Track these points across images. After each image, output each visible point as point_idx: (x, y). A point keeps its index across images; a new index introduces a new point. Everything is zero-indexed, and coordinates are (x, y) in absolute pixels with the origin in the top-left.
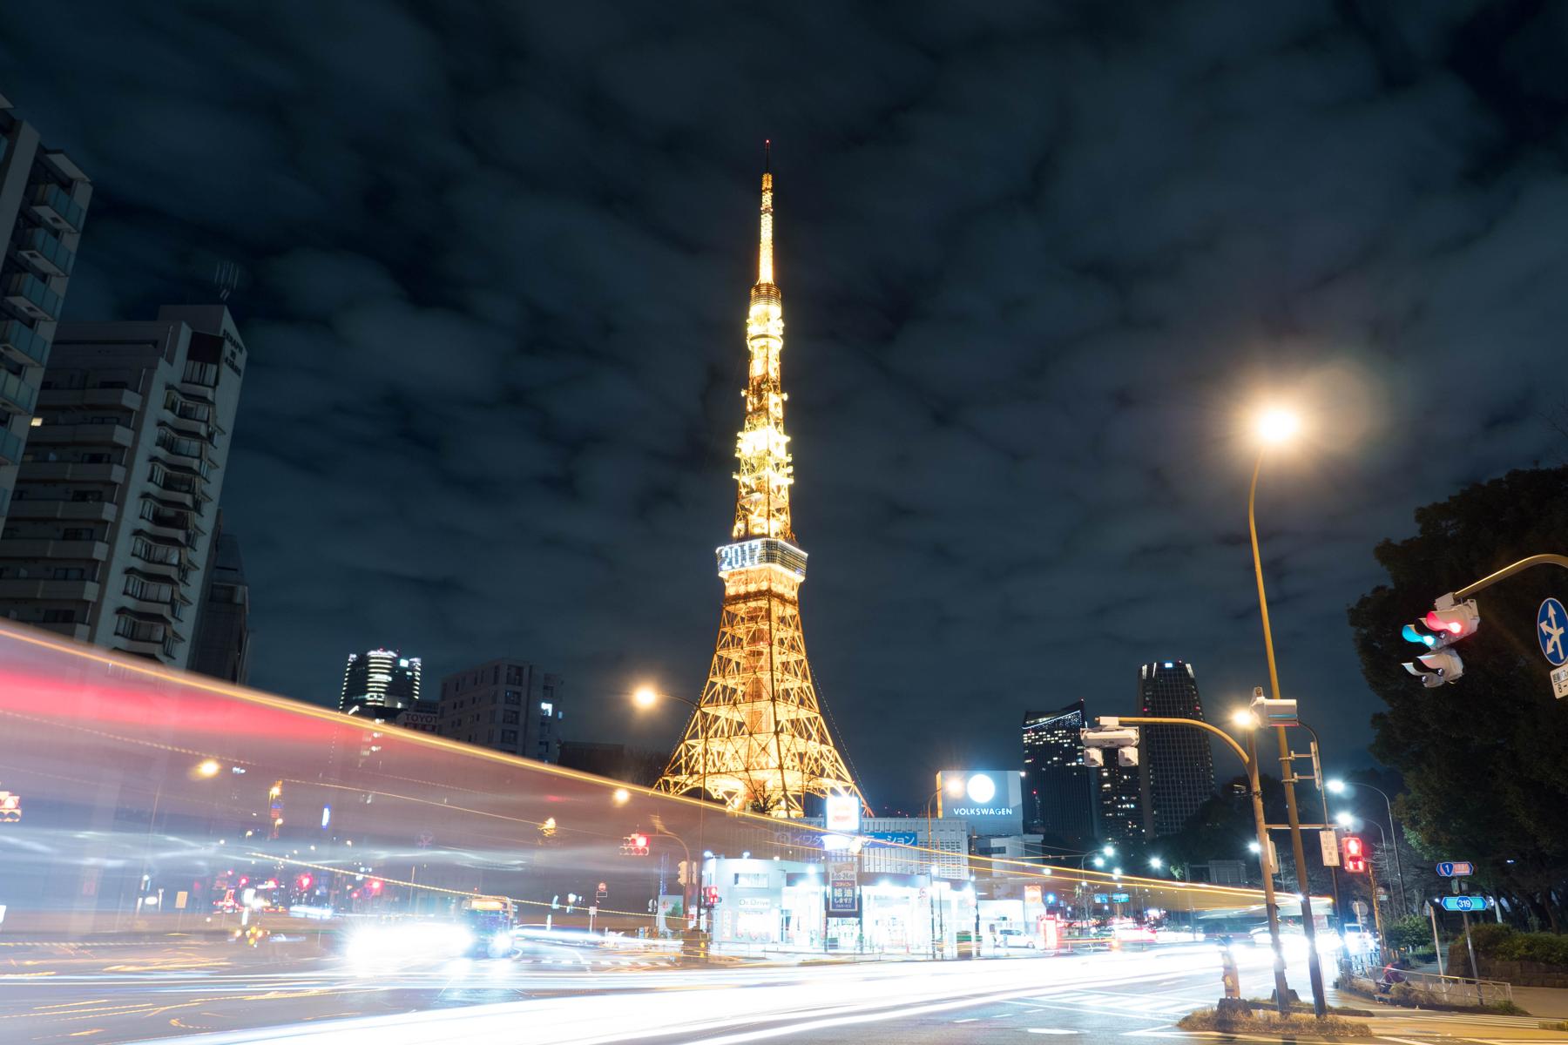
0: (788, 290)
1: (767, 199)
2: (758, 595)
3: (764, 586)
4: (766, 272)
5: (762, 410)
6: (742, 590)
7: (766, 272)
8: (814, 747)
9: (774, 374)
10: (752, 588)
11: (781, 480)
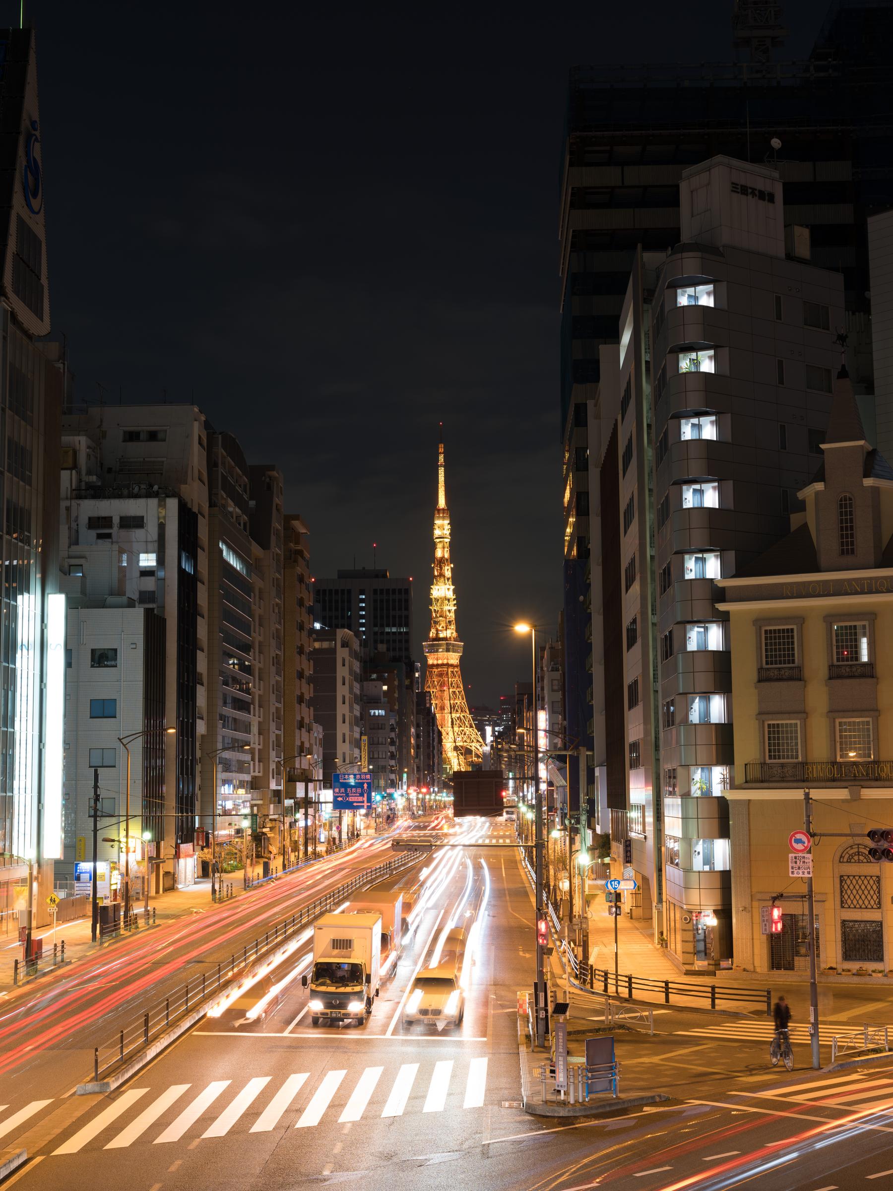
0: (454, 512)
1: (441, 458)
2: (443, 665)
3: (445, 662)
4: (442, 502)
5: (442, 575)
6: (435, 662)
7: (442, 502)
8: (468, 730)
9: (447, 555)
10: (440, 662)
11: (450, 608)
